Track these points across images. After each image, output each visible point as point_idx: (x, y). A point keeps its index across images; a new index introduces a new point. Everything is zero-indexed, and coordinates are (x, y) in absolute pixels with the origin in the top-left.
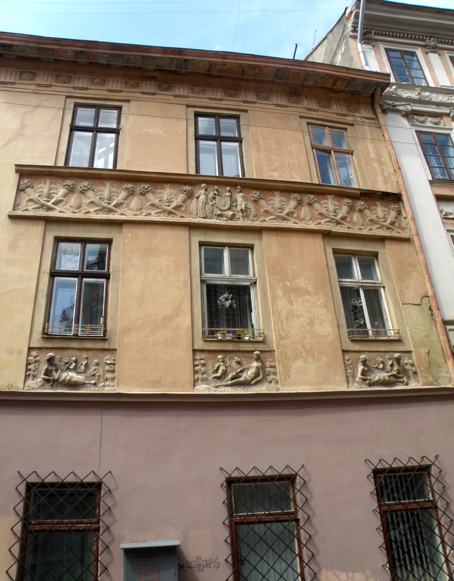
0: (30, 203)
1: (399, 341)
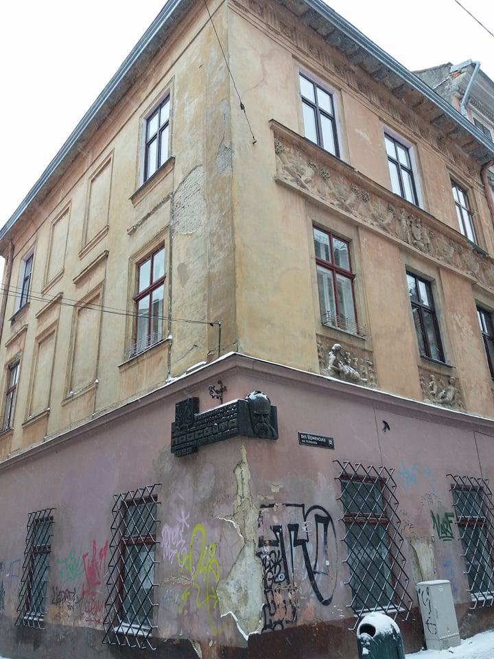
0: (286, 172)
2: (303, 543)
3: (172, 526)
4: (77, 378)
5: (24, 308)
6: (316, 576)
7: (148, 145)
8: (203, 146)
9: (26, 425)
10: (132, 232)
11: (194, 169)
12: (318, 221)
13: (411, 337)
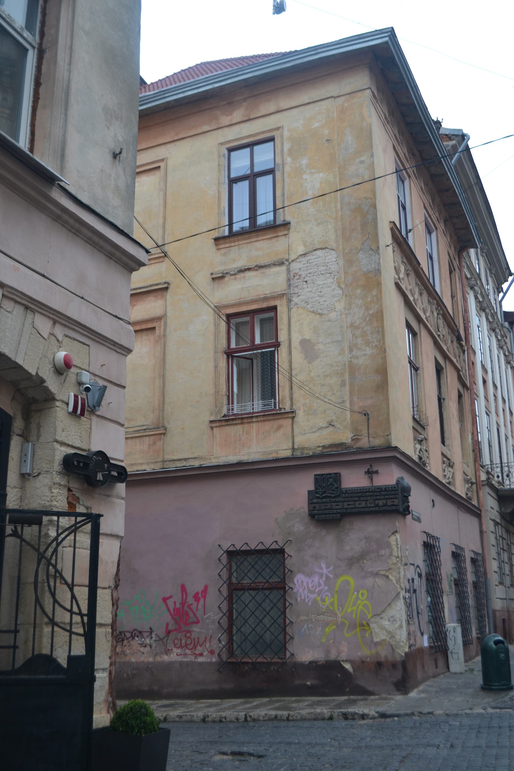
8: (336, 231)
11: (322, 249)
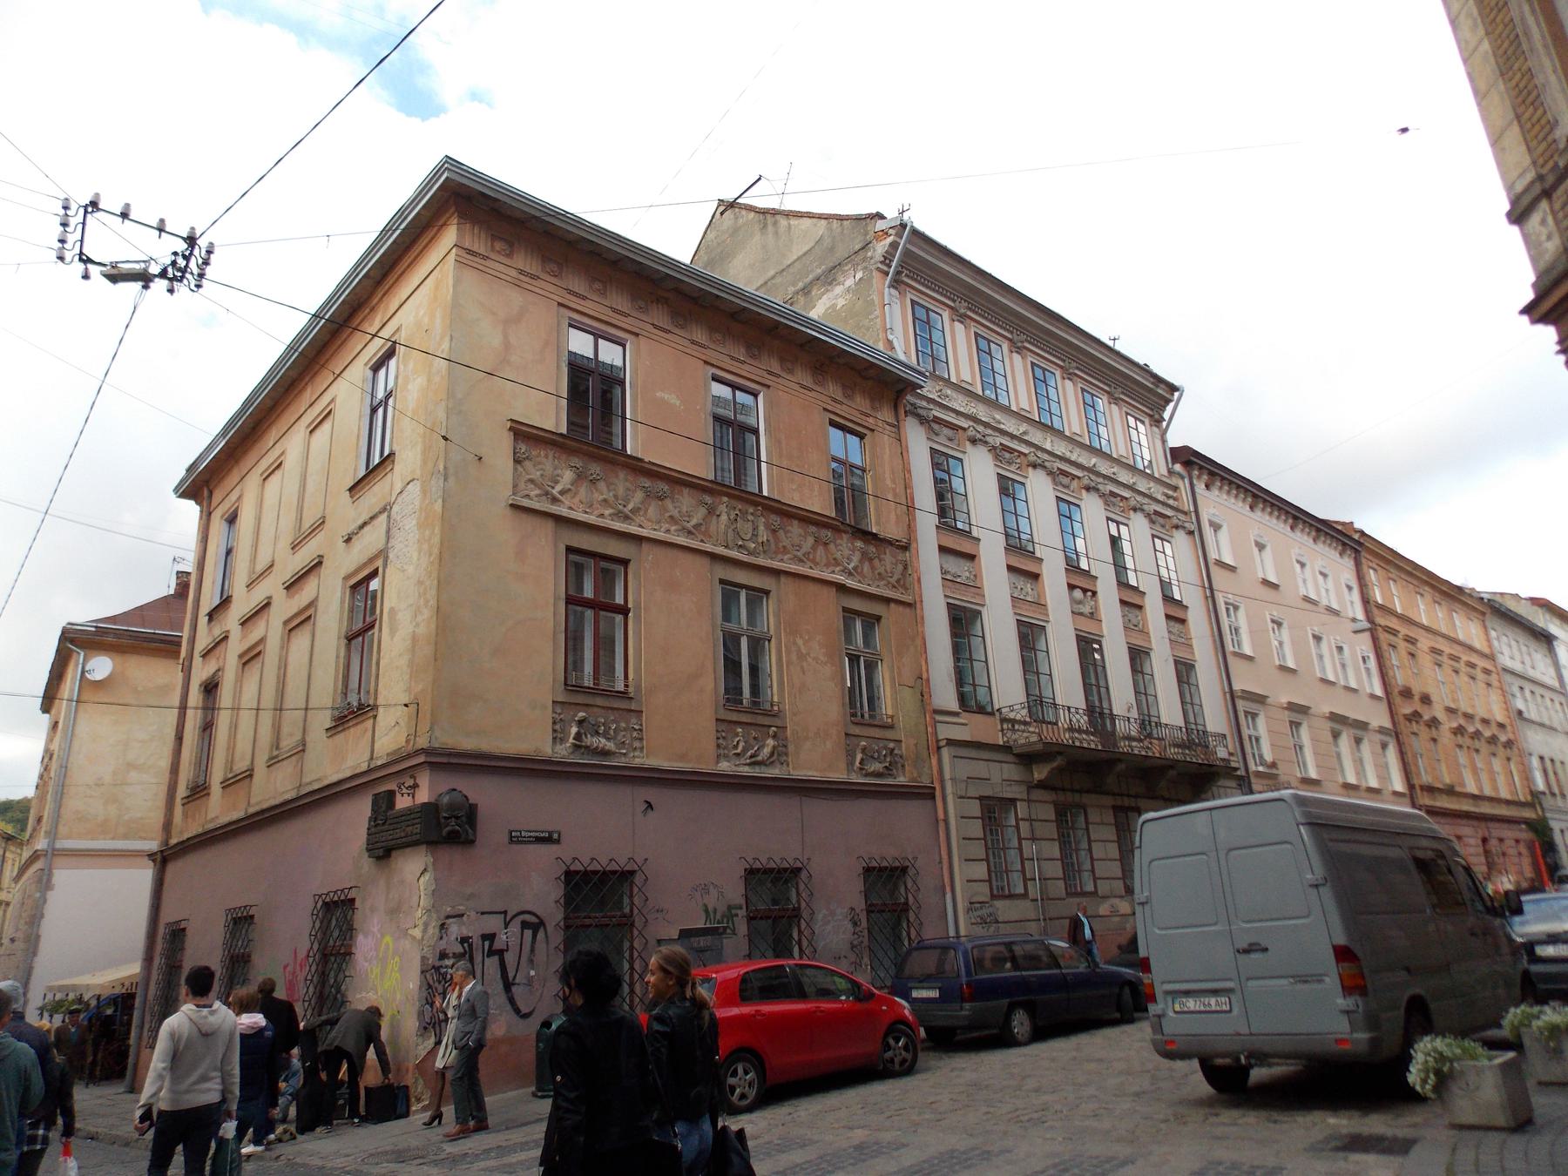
1: (891, 727)
2: (500, 953)
3: (366, 937)
4: (285, 729)
5: (225, 602)
6: (514, 989)
7: (374, 410)
9: (227, 784)
10: (348, 540)
12: (575, 545)
13: (711, 682)
